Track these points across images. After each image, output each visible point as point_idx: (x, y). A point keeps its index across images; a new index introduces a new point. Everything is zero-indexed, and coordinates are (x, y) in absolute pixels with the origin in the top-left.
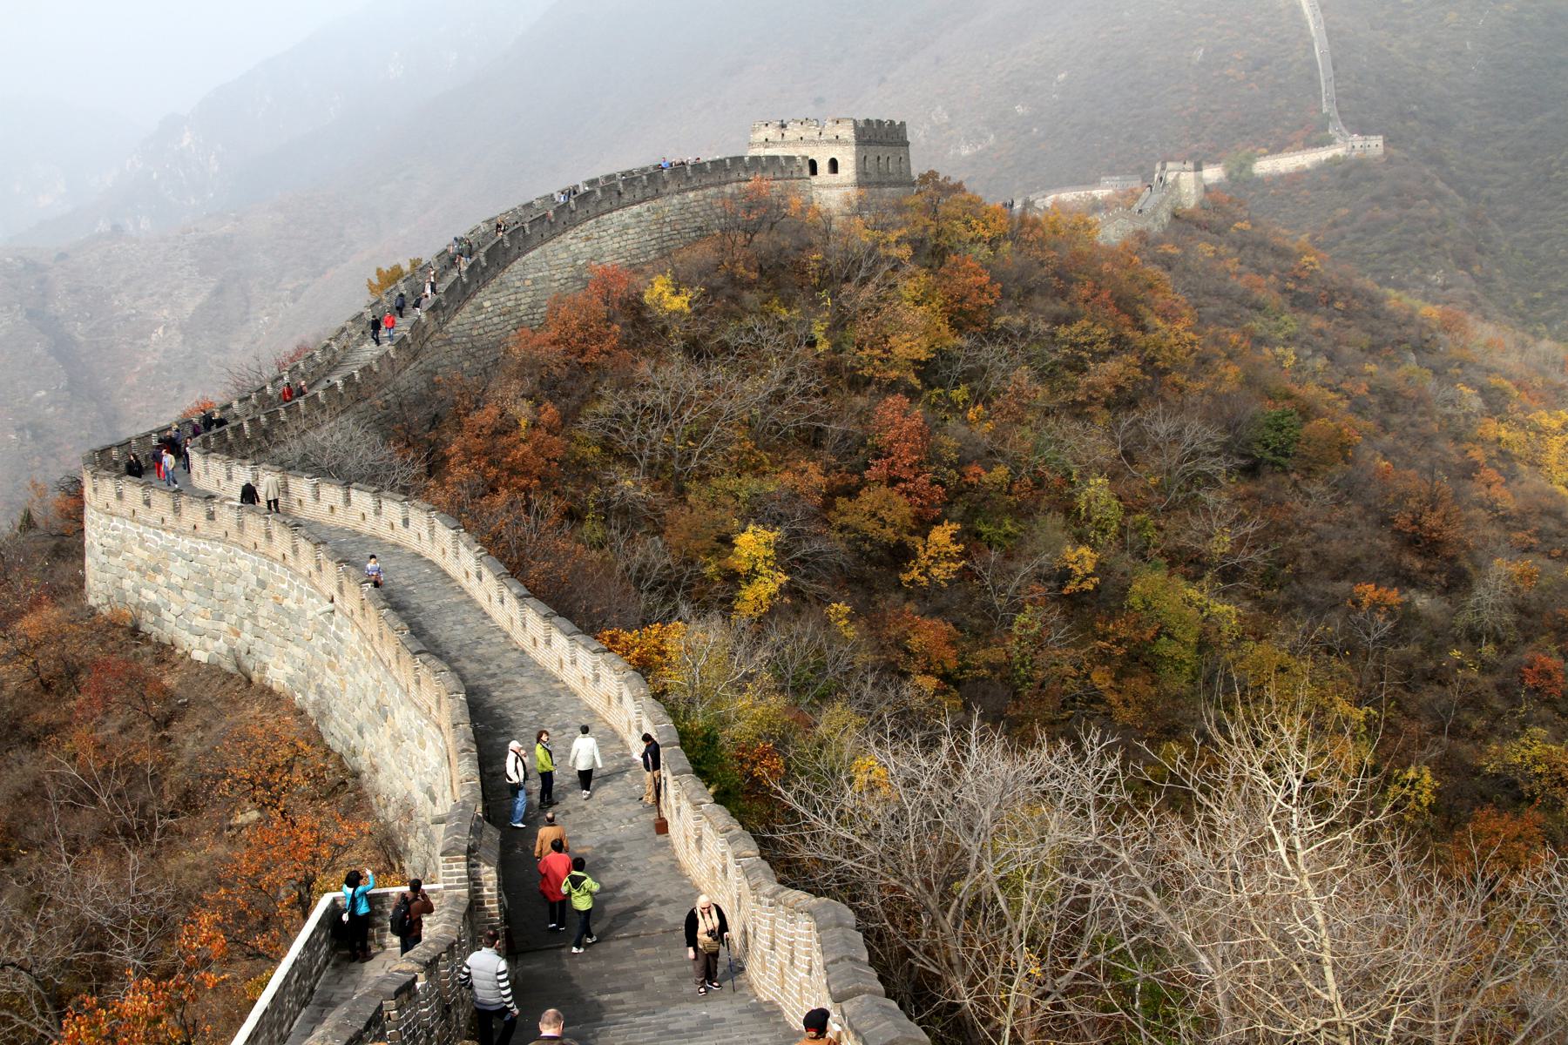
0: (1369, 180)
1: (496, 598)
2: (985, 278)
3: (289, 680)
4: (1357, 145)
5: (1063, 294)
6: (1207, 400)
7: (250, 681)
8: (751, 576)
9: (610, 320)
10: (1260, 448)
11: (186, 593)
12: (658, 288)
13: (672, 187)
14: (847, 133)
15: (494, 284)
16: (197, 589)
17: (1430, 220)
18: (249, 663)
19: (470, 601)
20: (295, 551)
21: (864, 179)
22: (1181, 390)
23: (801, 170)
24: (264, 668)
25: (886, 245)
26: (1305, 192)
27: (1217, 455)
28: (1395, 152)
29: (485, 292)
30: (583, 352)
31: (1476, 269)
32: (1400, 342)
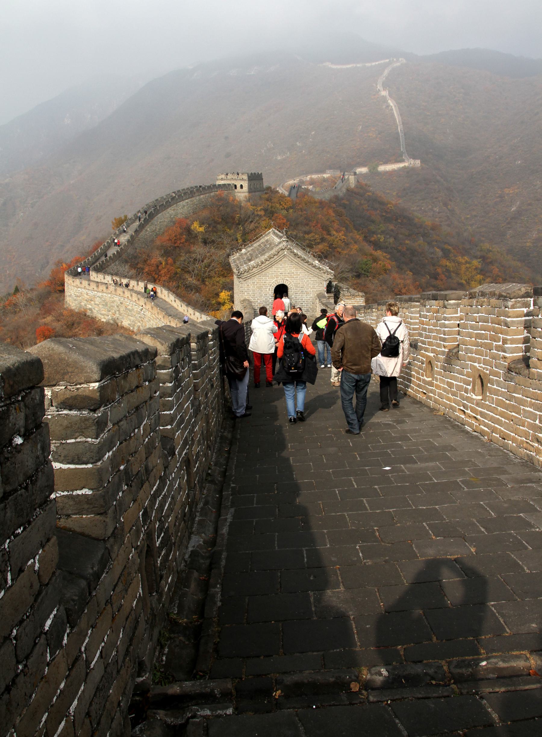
1: (180, 306)
2: (285, 221)
3: (129, 324)
4: (412, 162)
5: (307, 225)
6: (347, 256)
7: (118, 325)
8: (223, 304)
9: (181, 234)
10: (360, 270)
11: (100, 306)
12: (195, 225)
13: (197, 194)
14: (245, 177)
15: (150, 224)
16: (103, 305)
18: (118, 321)
19: (173, 306)
20: (131, 295)
21: (250, 191)
22: (340, 253)
23: (232, 188)
24: (122, 322)
25: (257, 211)
26: (395, 178)
27: (348, 272)
29: (148, 226)
30: (175, 243)
31: (449, 207)
32: (418, 234)
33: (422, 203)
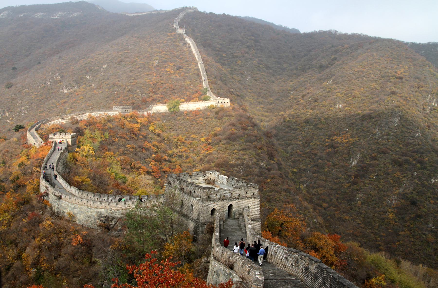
0: (227, 116)
17: (256, 136)
28: (233, 105)
33: (244, 155)
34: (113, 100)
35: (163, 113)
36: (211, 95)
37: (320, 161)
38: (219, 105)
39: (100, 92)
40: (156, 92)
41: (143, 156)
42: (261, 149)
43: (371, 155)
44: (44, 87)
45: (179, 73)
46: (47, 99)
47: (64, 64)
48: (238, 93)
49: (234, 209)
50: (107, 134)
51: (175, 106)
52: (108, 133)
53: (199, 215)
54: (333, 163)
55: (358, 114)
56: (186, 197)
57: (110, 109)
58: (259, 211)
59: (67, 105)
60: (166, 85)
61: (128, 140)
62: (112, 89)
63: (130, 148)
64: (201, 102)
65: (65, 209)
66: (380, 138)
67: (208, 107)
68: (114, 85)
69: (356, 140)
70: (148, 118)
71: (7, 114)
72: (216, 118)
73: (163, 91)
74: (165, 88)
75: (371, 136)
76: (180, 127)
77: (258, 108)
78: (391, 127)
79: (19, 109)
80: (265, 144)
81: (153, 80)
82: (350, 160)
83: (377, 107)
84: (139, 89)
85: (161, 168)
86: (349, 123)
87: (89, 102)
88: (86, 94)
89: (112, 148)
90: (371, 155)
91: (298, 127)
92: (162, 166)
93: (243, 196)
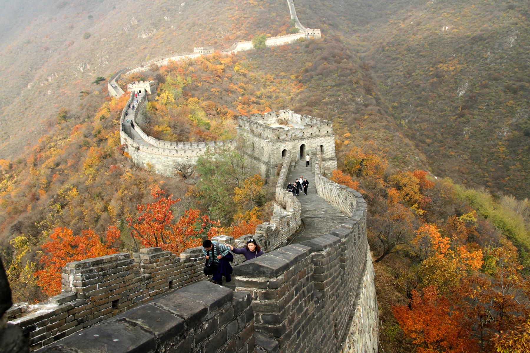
0: (318, 49)
4: (310, 33)
17: (351, 70)
28: (325, 37)
34: (195, 41)
35: (248, 51)
36: (299, 26)
37: (423, 93)
38: (309, 37)
39: (180, 33)
40: (240, 28)
41: (229, 99)
42: (356, 83)
43: (481, 83)
44: (122, 34)
45: (263, 4)
46: (127, 46)
47: (139, 6)
48: (330, 22)
49: (307, 149)
50: (189, 79)
51: (261, 42)
52: (190, 78)
53: (269, 158)
54: (438, 94)
55: (468, 37)
56: (256, 139)
57: (191, 51)
58: (334, 150)
59: (146, 51)
60: (250, 19)
61: (212, 84)
62: (192, 29)
63: (215, 92)
64: (289, 35)
65: (144, 160)
66: (491, 62)
67: (297, 40)
68: (194, 24)
69: (463, 67)
70: (232, 58)
71: (89, 67)
72: (306, 52)
73: (247, 26)
74: (249, 23)
75: (481, 60)
76: (267, 64)
77: (354, 37)
78: (505, 48)
79: (100, 60)
80: (361, 78)
81: (235, 15)
82: (457, 90)
83: (490, 26)
84: (221, 26)
85: (249, 111)
86: (457, 47)
87: (169, 46)
88: (166, 37)
89: (196, 93)
90: (481, 83)
91: (398, 56)
92: (250, 109)
93: (316, 135)
